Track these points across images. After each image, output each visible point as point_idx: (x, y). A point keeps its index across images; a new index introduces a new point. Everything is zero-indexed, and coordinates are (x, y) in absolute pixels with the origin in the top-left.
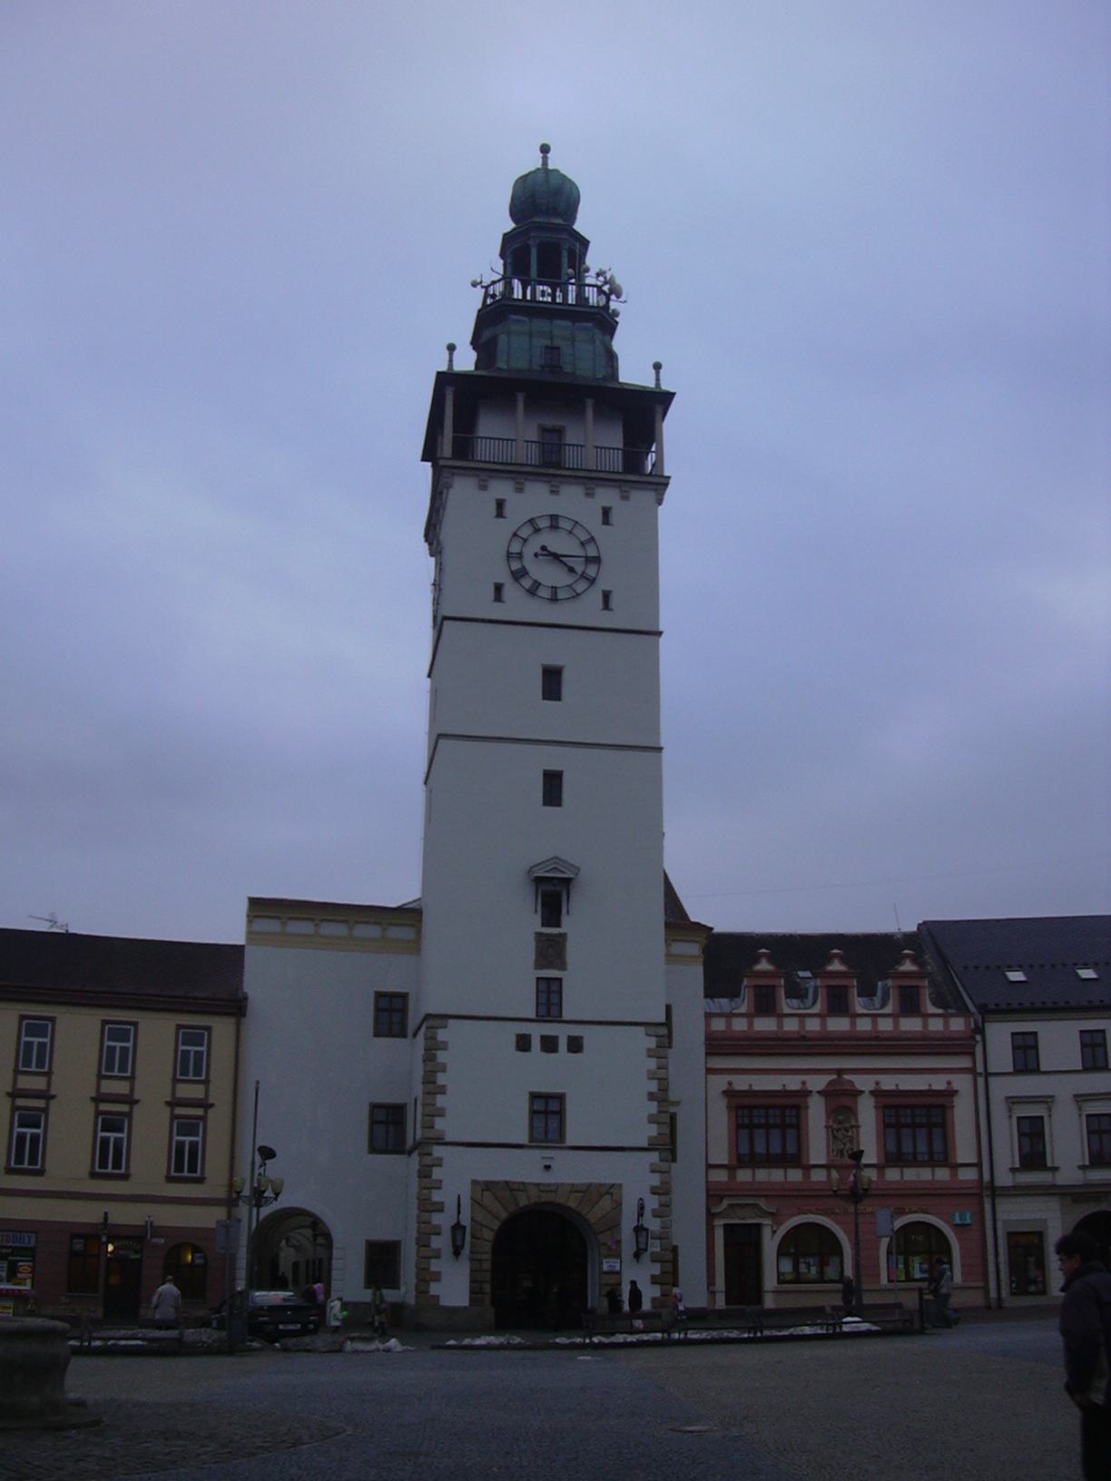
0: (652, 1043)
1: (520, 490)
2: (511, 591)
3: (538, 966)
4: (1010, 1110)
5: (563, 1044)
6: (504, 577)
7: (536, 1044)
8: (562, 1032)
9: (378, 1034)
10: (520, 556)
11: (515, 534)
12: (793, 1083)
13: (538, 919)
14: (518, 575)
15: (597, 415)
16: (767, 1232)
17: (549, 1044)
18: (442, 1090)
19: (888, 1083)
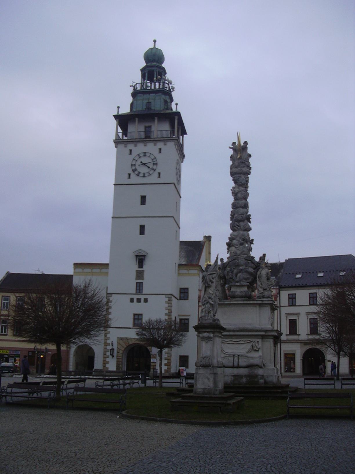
0: (167, 299)
2: (133, 175)
3: (137, 279)
4: (287, 317)
5: (142, 300)
6: (131, 172)
7: (135, 300)
8: (142, 297)
10: (135, 165)
13: (137, 266)
14: (134, 171)
15: (158, 121)
17: (139, 300)
18: (110, 313)
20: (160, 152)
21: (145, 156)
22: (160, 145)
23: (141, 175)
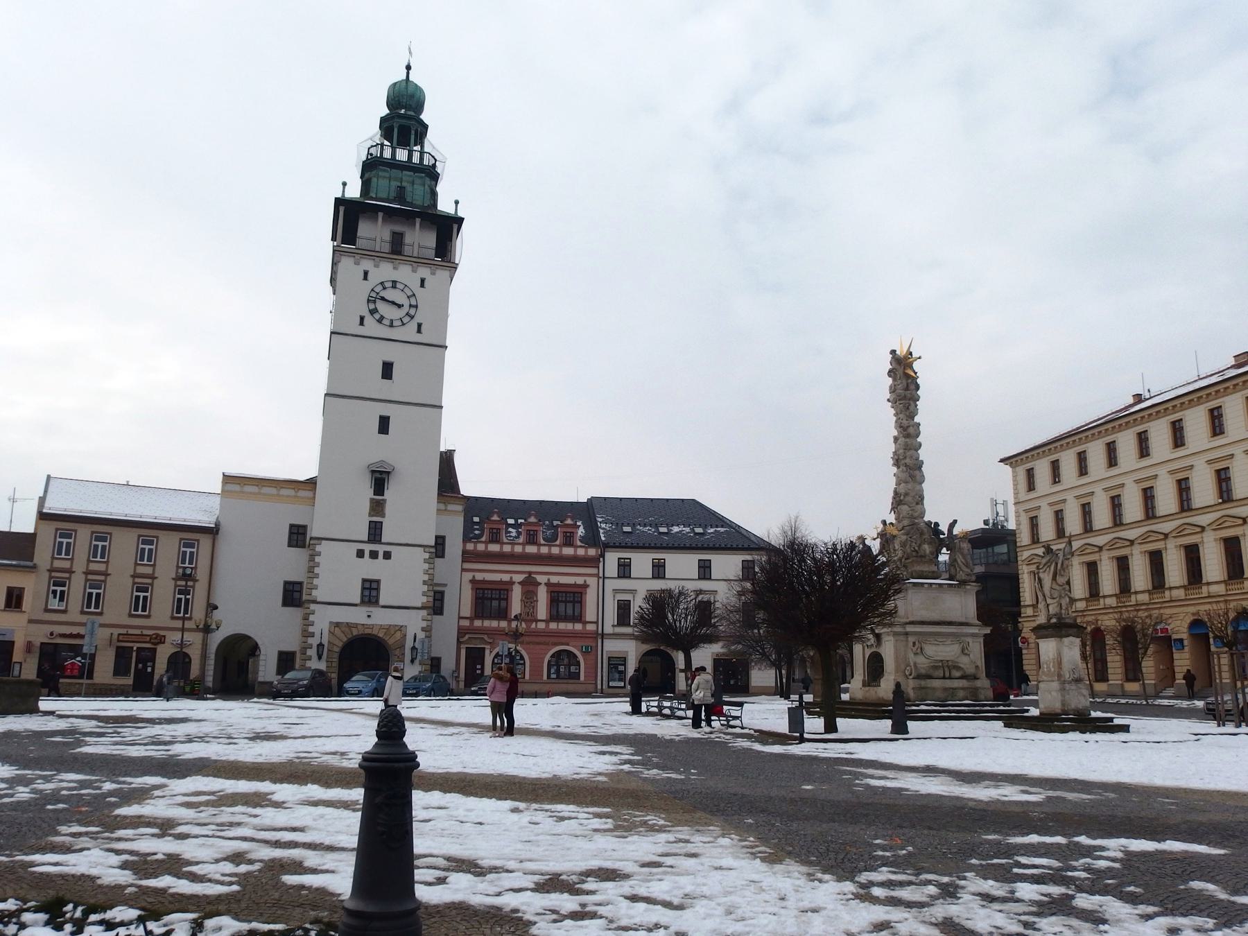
0: (427, 556)
1: (376, 266)
2: (369, 320)
3: (370, 515)
5: (381, 555)
7: (367, 554)
9: (290, 545)
12: (506, 577)
16: (487, 652)
17: (374, 555)
18: (317, 576)
19: (554, 579)
20: (422, 285)
21: (394, 287)
23: (386, 322)
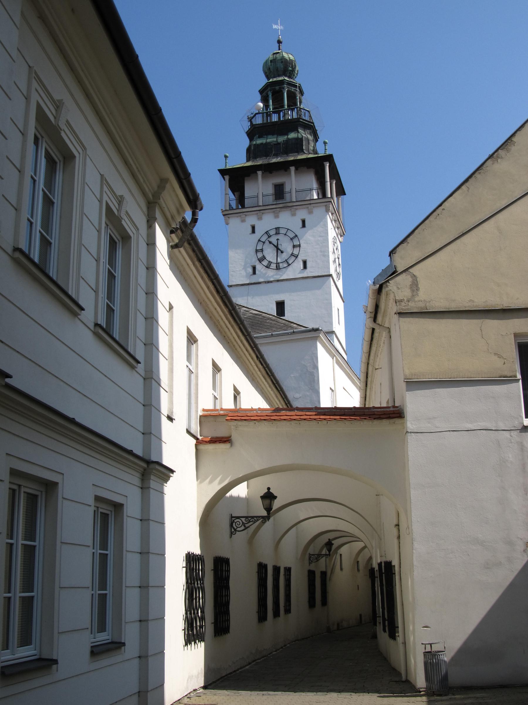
2: (259, 267)
11: (259, 240)
20: (304, 225)
22: (302, 214)
